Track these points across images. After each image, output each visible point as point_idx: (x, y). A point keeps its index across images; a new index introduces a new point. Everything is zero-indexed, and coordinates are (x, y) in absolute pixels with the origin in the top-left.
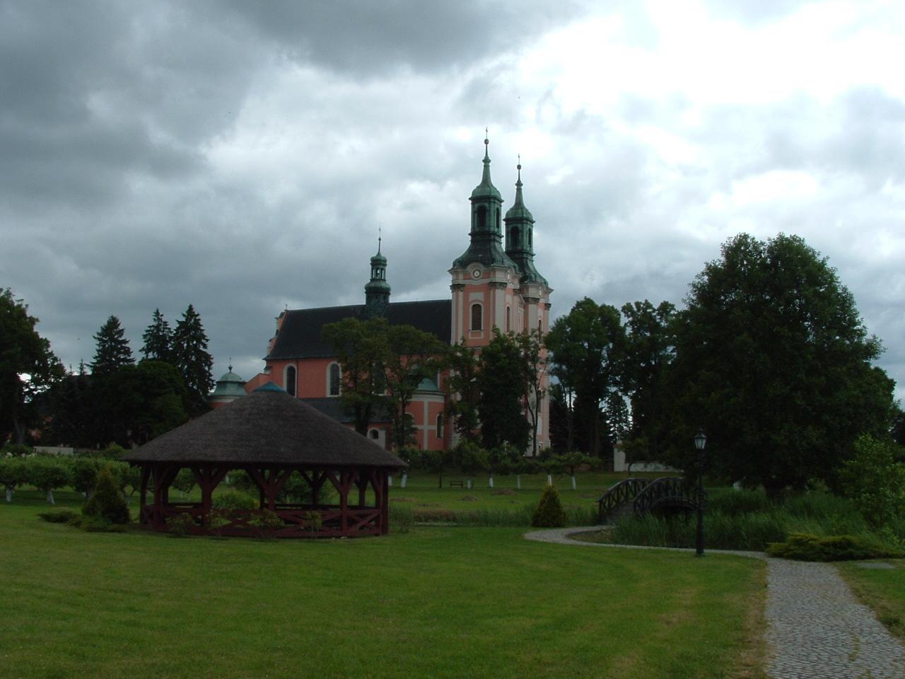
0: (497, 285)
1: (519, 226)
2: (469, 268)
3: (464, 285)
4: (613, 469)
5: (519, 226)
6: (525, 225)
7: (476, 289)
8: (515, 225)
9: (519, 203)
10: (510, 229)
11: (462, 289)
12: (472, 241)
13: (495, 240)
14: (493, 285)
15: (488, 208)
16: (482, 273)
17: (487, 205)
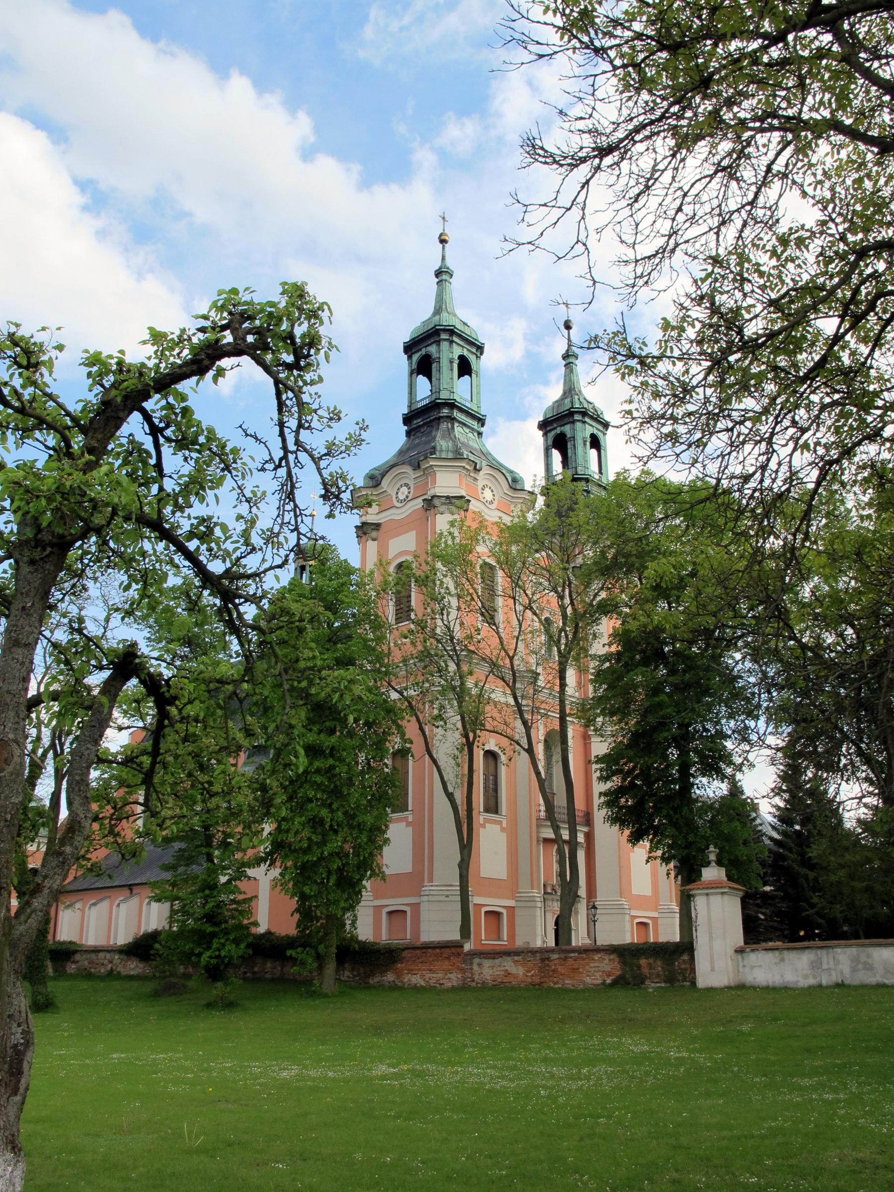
0: (436, 502)
1: (567, 429)
2: (385, 483)
3: (377, 526)
4: (693, 983)
5: (567, 429)
6: (578, 425)
7: (400, 527)
8: (558, 431)
9: (570, 390)
10: (550, 442)
11: (374, 534)
12: (408, 434)
13: (453, 419)
14: (430, 504)
15: (435, 355)
16: (412, 490)
17: (432, 349)
